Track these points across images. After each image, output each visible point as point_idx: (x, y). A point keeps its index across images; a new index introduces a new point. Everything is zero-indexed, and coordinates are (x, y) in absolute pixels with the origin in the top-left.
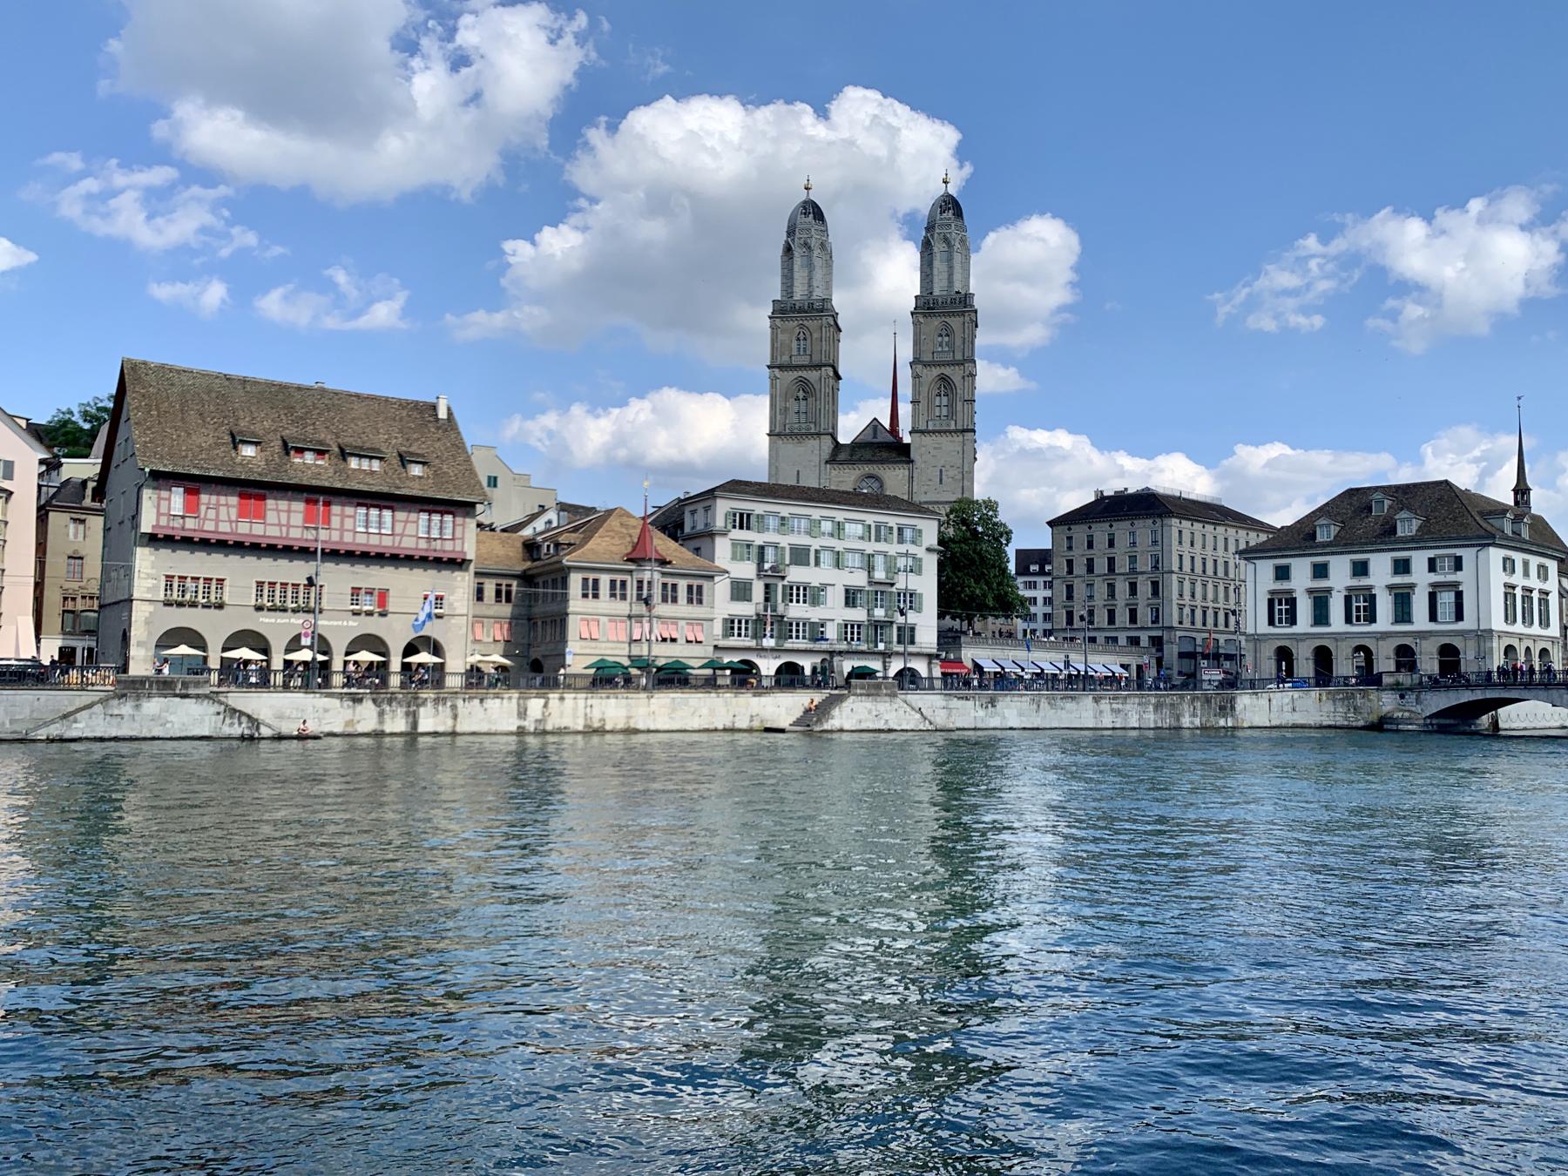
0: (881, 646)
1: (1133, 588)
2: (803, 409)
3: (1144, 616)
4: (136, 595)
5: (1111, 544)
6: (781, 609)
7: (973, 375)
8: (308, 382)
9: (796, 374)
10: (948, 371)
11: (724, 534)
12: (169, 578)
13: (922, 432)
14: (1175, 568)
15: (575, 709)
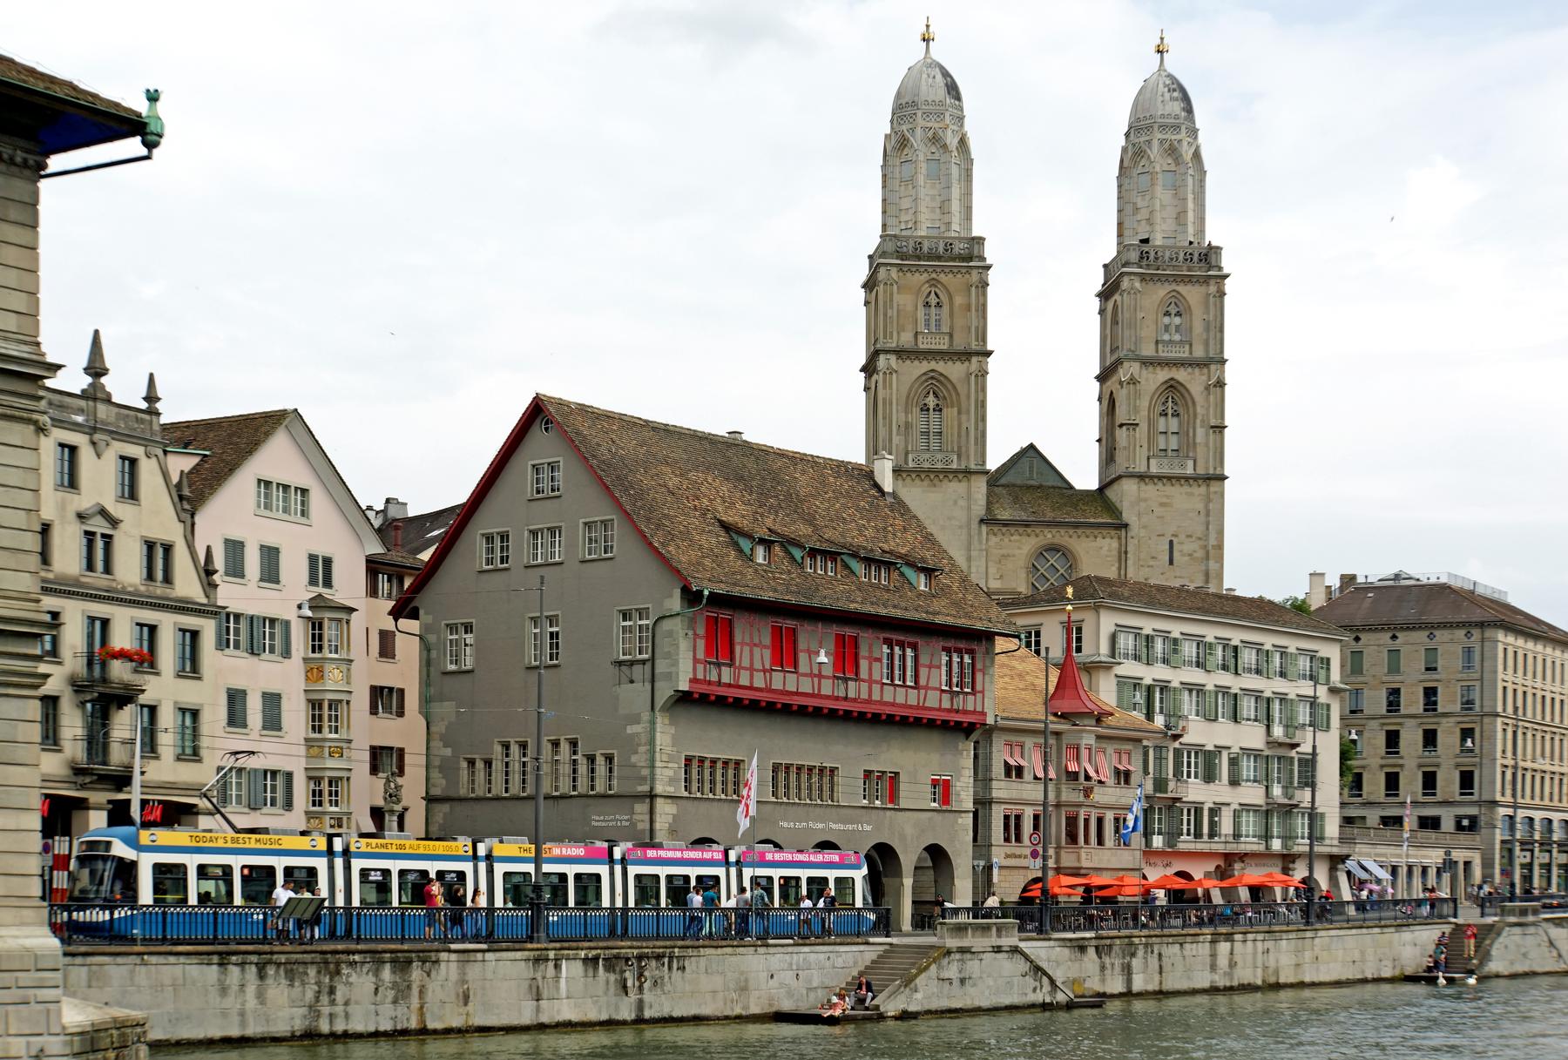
0: (1276, 845)
1: (1430, 738)
2: (934, 428)
3: (1448, 782)
4: (659, 789)
5: (1394, 668)
6: (1171, 785)
7: (1221, 384)
8: (720, 429)
9: (925, 366)
10: (1181, 375)
11: (1107, 667)
12: (688, 760)
13: (1142, 477)
14: (1500, 709)
15: (1255, 953)
